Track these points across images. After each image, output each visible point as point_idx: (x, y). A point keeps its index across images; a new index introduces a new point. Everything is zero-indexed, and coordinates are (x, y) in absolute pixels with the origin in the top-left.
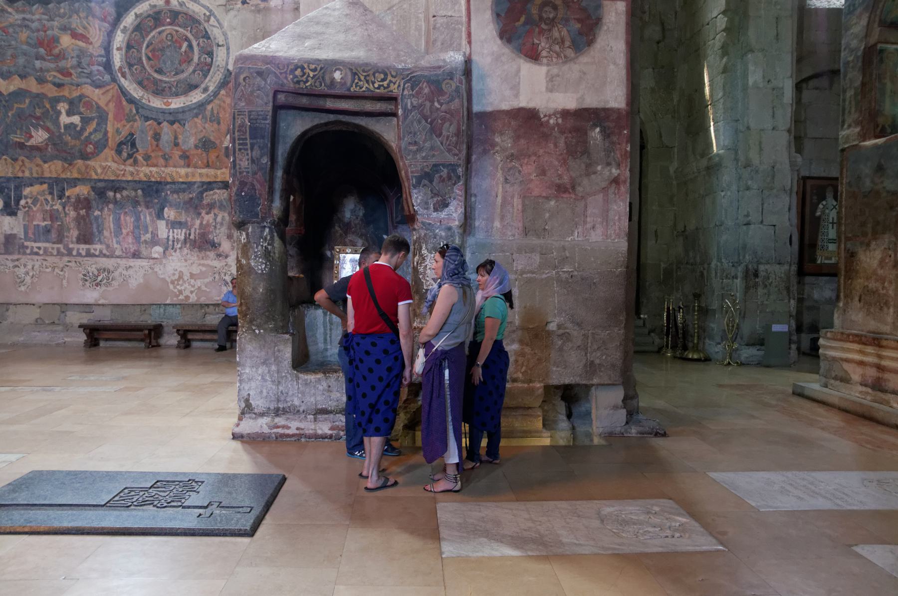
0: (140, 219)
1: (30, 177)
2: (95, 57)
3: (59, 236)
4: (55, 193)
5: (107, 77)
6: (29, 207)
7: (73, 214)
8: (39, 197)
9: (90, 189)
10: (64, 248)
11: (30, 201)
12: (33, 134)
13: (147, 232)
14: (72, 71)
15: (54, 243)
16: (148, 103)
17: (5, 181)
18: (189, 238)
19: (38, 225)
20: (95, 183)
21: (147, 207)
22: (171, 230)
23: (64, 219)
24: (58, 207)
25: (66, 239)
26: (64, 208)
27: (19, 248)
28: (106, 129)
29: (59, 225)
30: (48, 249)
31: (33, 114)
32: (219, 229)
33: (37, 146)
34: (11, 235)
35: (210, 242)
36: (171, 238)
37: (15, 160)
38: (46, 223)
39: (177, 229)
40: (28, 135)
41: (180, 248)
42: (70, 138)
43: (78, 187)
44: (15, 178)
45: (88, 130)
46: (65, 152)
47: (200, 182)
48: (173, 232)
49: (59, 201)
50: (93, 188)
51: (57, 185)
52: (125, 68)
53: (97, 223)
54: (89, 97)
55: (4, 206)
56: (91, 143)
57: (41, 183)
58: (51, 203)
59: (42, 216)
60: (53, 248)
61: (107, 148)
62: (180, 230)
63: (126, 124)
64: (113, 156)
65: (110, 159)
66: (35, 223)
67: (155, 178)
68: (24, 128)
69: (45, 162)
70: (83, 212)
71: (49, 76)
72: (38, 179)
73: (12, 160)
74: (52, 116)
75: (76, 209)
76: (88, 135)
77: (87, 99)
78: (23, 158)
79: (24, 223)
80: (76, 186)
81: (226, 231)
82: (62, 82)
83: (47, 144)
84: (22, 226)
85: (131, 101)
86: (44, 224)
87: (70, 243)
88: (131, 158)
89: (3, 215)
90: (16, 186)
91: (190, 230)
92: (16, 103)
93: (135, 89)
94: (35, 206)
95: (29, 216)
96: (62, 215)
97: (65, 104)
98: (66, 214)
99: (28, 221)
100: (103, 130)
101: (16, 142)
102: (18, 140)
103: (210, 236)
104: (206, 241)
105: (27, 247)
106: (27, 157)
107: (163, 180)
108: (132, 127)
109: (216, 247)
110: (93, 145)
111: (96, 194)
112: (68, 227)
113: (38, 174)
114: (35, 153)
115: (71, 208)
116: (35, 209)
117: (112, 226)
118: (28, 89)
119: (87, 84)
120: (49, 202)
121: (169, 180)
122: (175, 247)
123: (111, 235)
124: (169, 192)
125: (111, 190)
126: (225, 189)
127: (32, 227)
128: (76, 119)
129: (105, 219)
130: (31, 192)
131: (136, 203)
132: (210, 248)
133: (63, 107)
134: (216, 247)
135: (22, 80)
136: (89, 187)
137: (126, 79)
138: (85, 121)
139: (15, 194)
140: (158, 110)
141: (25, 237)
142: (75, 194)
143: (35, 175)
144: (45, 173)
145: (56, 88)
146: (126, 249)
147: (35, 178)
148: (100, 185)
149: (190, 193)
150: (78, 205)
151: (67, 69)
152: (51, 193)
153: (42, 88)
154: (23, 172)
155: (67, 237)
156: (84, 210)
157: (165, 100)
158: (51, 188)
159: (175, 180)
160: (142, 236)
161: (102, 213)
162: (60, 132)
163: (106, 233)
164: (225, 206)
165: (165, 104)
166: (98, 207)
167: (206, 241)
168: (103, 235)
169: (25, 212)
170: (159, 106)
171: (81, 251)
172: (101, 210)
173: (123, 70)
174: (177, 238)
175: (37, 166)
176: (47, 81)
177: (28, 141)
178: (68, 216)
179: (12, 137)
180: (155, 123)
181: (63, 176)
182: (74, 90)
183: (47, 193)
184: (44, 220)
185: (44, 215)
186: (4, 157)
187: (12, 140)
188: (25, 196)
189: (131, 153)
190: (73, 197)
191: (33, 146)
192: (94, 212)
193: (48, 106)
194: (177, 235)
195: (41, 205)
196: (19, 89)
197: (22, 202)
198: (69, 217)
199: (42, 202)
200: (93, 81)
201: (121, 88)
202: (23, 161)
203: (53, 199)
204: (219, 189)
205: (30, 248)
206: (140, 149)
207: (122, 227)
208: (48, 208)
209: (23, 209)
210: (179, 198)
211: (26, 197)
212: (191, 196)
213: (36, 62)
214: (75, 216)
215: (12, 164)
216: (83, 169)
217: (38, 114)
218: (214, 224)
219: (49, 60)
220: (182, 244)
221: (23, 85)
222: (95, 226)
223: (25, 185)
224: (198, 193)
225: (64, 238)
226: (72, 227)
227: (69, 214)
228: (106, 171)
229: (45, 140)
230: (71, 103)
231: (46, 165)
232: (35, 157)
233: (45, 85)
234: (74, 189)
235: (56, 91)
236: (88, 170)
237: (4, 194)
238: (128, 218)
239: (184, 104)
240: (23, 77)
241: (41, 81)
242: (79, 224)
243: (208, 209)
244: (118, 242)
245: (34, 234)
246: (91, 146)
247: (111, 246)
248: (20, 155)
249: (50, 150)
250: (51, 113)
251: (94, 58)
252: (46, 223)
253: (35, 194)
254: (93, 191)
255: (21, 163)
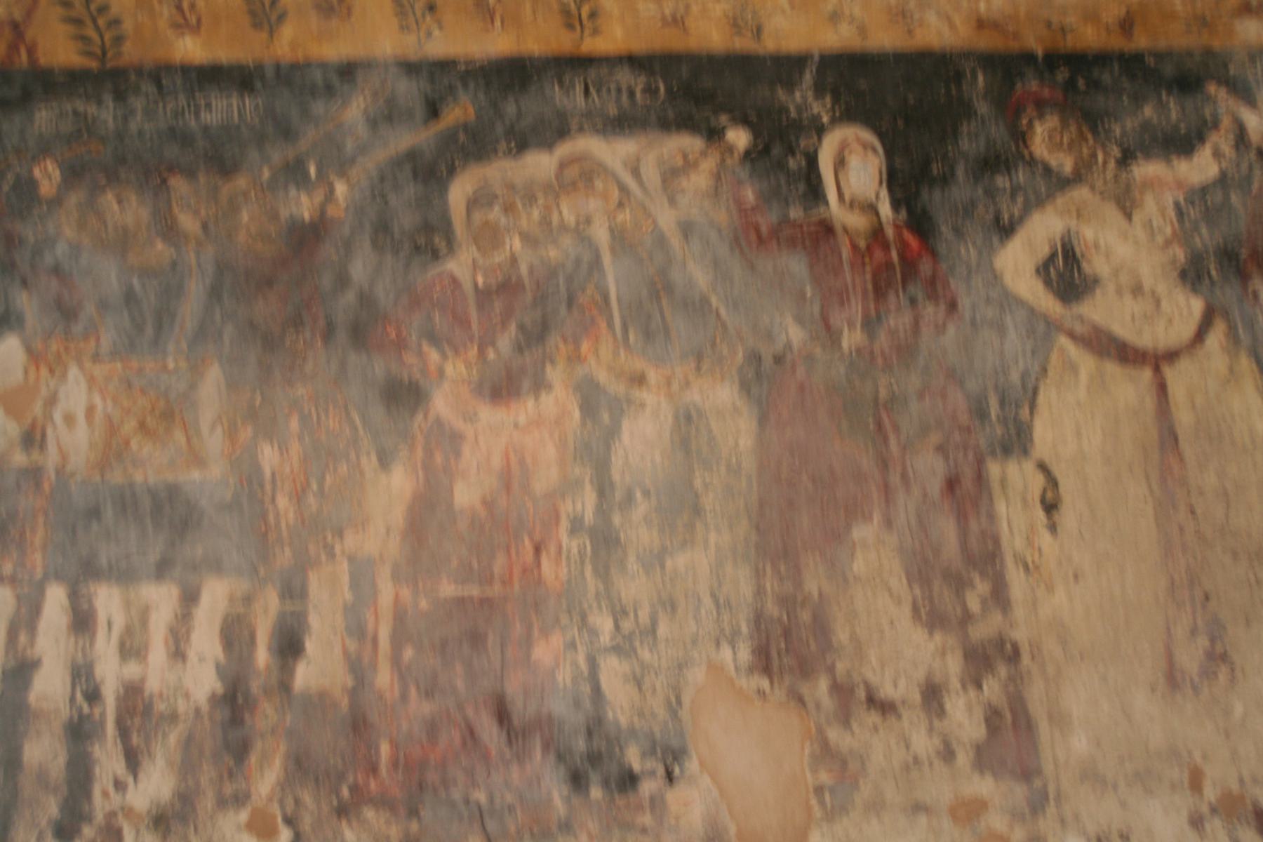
18: (285, 686)
22: (56, 598)
32: (655, 560)
35: (545, 726)
39: (125, 576)
47: (410, 68)
48: (82, 622)
81: (741, 583)
91: (294, 591)
103: (543, 652)
104: (502, 715)
109: (629, 780)
122: (100, 803)
124: (48, 176)
126: (685, 123)
132: (556, 792)
134: (629, 780)
149: (294, 172)
159: (130, 53)
164: (698, 308)
167: (502, 715)
174: (132, 694)
194: (131, 649)
204: (621, 124)
210: (169, 230)
212: (303, 206)
218: (587, 503)
220: (187, 766)
224: (385, 180)
243: (505, 342)
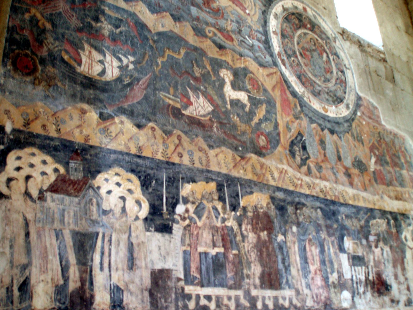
0: (324, 251)
1: (191, 166)
2: (254, 30)
3: (236, 274)
4: (227, 200)
5: (268, 58)
6: (191, 219)
7: (252, 237)
8: (205, 202)
9: (270, 200)
10: (245, 298)
11: (191, 208)
12: (192, 99)
13: (332, 272)
14: (233, 36)
15: (230, 288)
16: (308, 102)
17: (152, 165)
19: (206, 254)
20: (274, 192)
21: (329, 235)
23: (242, 244)
24: (231, 223)
25: (247, 281)
26: (240, 225)
27: (177, 300)
28: (276, 120)
29: (235, 255)
30: (223, 299)
31: (191, 72)
33: (199, 120)
34: (162, 271)
36: (354, 278)
37: (168, 133)
38: (217, 250)
39: (357, 266)
40: (185, 100)
41: (364, 293)
42: (238, 119)
43: (255, 194)
44: (167, 163)
45: (257, 115)
46: (235, 137)
49: (233, 213)
50: (273, 198)
51: (228, 186)
52: (283, 56)
53: (282, 254)
54: (253, 74)
55: (150, 213)
56: (262, 134)
57: (208, 180)
58: (222, 215)
59: (211, 237)
60: (229, 298)
61: (280, 145)
62: (360, 268)
63: (294, 120)
64: (287, 157)
65: (285, 161)
66: (201, 249)
67: (330, 196)
68: (179, 87)
69: (211, 147)
70: (264, 235)
71: (209, 31)
72: (202, 172)
73: (164, 132)
74: (214, 82)
75: (255, 230)
76: (258, 121)
77: (252, 75)
78: (180, 133)
79: (184, 248)
80: (252, 193)
82: (222, 43)
83: (210, 120)
84: (181, 255)
85: (294, 94)
86: (213, 252)
87: (252, 288)
88: (305, 164)
89: (148, 230)
90: (170, 178)
92: (169, 49)
93: (295, 82)
94: (200, 217)
95: (191, 235)
96: (239, 238)
97: (229, 72)
98: (242, 235)
99: (189, 245)
100: (274, 122)
101: (169, 105)
102: (171, 102)
105: (189, 297)
106: (186, 133)
107: (337, 200)
108: (300, 125)
110: (265, 138)
111: (276, 207)
112: (247, 259)
113: (201, 163)
114: (197, 130)
115: (249, 227)
116: (199, 224)
117: (298, 259)
118: (183, 36)
119: (251, 57)
120: (219, 214)
121: (342, 201)
123: (299, 275)
125: (291, 203)
127: (197, 256)
128: (242, 96)
129: (290, 248)
130: (193, 193)
131: (318, 228)
133: (227, 75)
135: (175, 22)
136: (267, 196)
137: (286, 68)
138: (255, 102)
139: (167, 192)
140: (315, 112)
141: (185, 275)
142: (252, 204)
143: (197, 165)
144: (211, 163)
145: (218, 50)
146: (317, 297)
147: (198, 170)
148: (280, 195)
150: (257, 223)
151: (228, 31)
152: (221, 199)
153: (200, 42)
154: (181, 156)
155: (248, 277)
156: (265, 232)
157: (323, 105)
158: (220, 188)
159: (347, 202)
160: (329, 275)
161: (285, 238)
162: (226, 108)
163: (294, 271)
165: (324, 108)
166: (280, 228)
168: (290, 274)
169: (185, 228)
170: (318, 109)
171: (267, 302)
172: (284, 234)
173: (282, 57)
175: (200, 151)
176: (206, 36)
177: (186, 108)
178: (246, 241)
179: (162, 94)
180: (319, 129)
181: (235, 174)
182: (237, 60)
183: (216, 197)
184: (214, 246)
185: (213, 236)
186: (151, 124)
187: (163, 101)
188: (183, 197)
189: (304, 157)
190: (250, 209)
191: (193, 118)
192: (276, 236)
193: (209, 68)
195: (208, 218)
196: (171, 31)
197: (180, 209)
198: (248, 242)
199: (209, 212)
200: (256, 58)
201: (282, 75)
202: (179, 138)
203: (224, 208)
205: (194, 297)
206: (311, 155)
207: (309, 261)
208: (219, 224)
209: (181, 222)
211: (186, 201)
213: (192, 7)
214: (255, 241)
215: (164, 138)
216: (258, 167)
217: (197, 74)
219: (206, 11)
221: (177, 29)
222: (280, 258)
223: (183, 178)
225: (243, 278)
226: (253, 259)
227: (247, 237)
228: (283, 175)
229: (209, 114)
230: (236, 73)
231: (212, 153)
232: (197, 136)
233: (205, 39)
234: (250, 196)
235: (217, 52)
236: (264, 171)
237: (151, 190)
238: (313, 248)
239: (336, 115)
240: (176, 19)
241: (199, 32)
242: (261, 254)
244: (308, 286)
245: (200, 270)
246: (263, 138)
247: (301, 292)
248: (174, 127)
249: (215, 130)
250: (213, 78)
251: (253, 32)
252: (217, 250)
253: (199, 196)
254: (273, 204)
255: (177, 141)
